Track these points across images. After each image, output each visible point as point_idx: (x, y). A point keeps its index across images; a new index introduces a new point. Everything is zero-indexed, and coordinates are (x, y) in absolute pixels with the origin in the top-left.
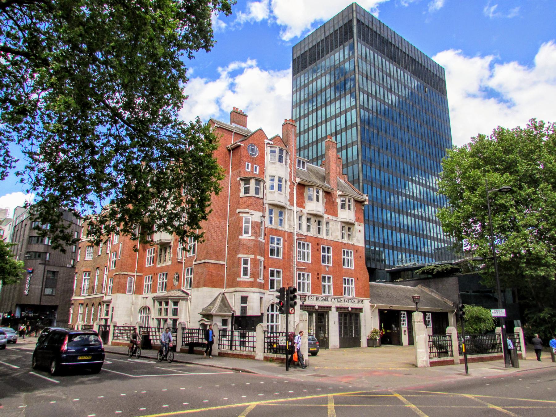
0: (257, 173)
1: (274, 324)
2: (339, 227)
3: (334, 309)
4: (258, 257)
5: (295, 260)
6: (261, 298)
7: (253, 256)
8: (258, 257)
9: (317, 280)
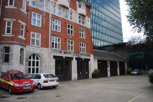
1: (35, 67)
2: (78, 17)
3: (74, 59)
4: (20, 21)
5: (50, 29)
6: (22, 50)
7: (15, 20)
8: (20, 21)
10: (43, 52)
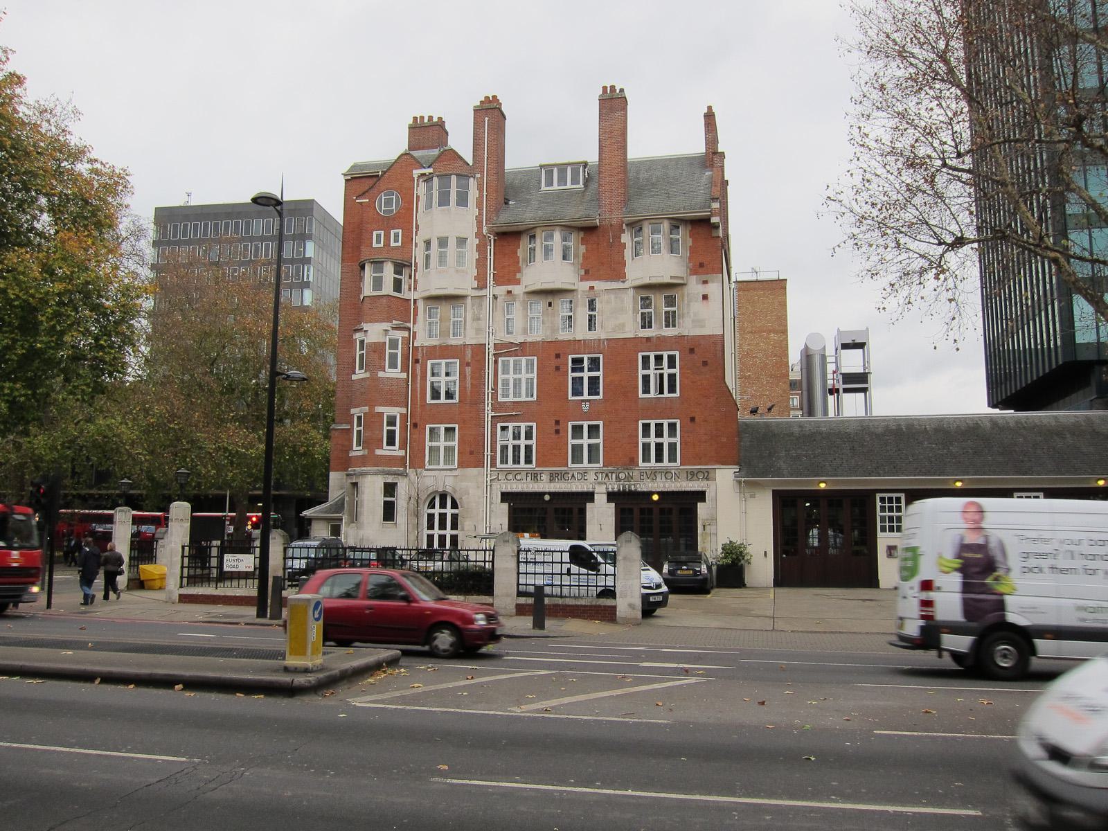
0: (399, 244)
1: (448, 532)
3: (601, 499)
4: (379, 409)
5: (489, 401)
8: (379, 409)
9: (554, 436)
10: (464, 484)
